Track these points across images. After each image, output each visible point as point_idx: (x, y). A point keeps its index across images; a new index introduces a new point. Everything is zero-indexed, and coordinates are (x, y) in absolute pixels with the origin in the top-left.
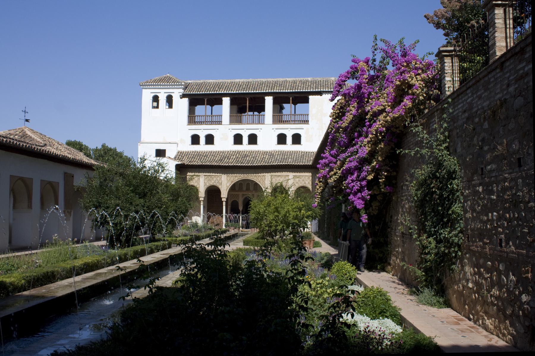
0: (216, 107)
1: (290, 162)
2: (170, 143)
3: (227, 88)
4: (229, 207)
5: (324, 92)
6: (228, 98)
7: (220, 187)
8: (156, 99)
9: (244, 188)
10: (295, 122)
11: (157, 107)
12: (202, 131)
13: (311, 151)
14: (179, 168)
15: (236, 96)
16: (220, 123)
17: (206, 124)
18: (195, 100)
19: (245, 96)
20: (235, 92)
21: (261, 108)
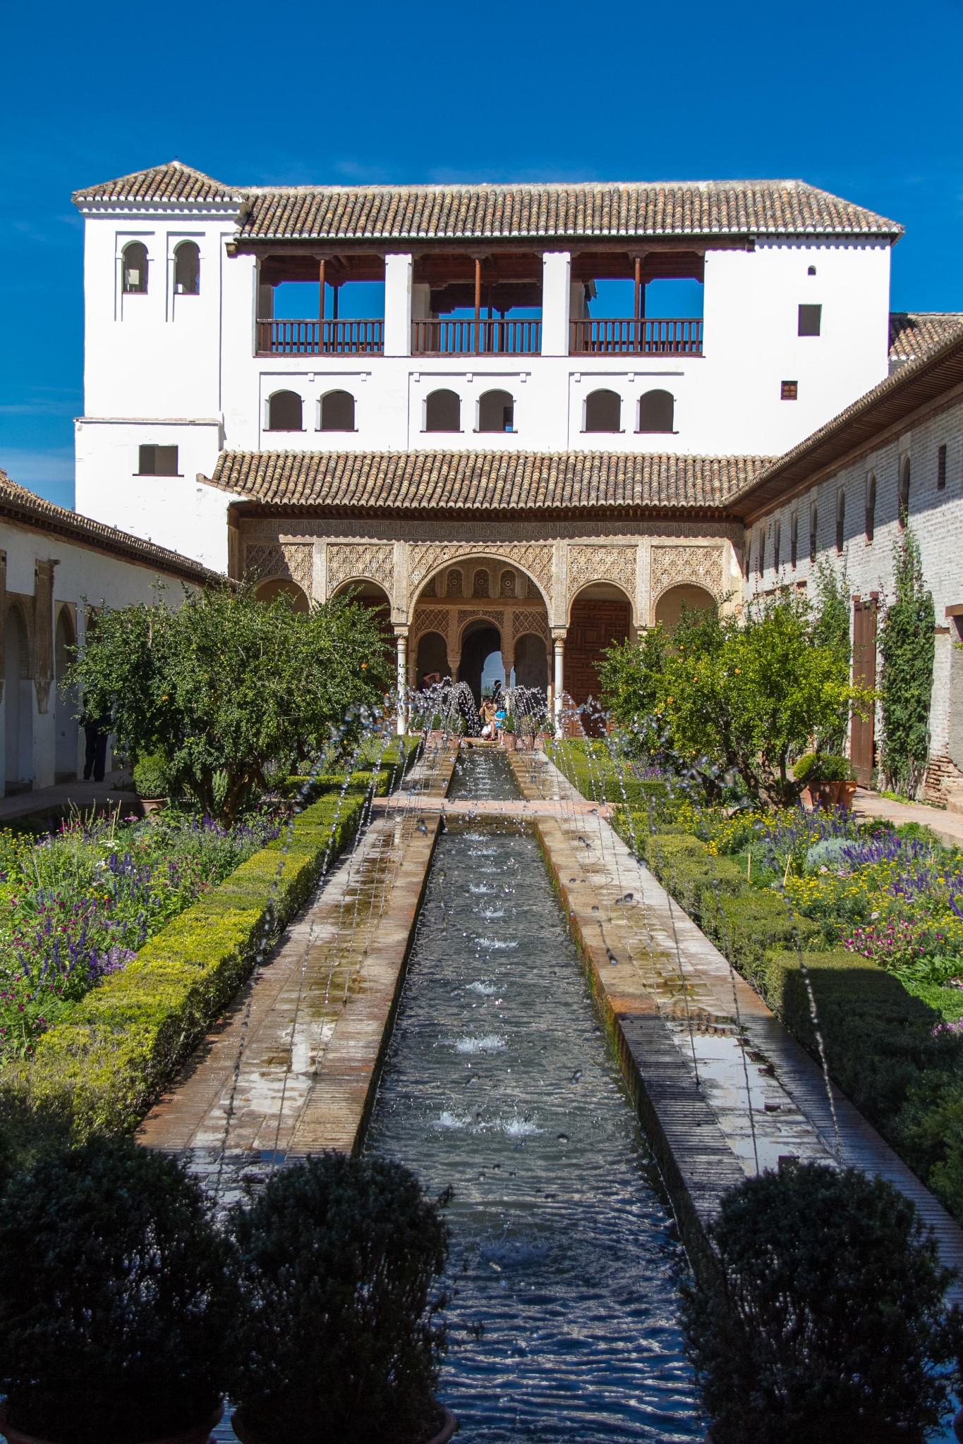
0: (348, 288)
1: (639, 495)
2: (192, 423)
3: (401, 217)
4: (413, 656)
5: (759, 235)
6: (408, 258)
7: (386, 586)
8: (135, 256)
9: (467, 591)
10: (644, 347)
11: (142, 288)
12: (311, 377)
13: (712, 456)
14: (241, 516)
15: (437, 251)
16: (374, 346)
17: (320, 354)
18: (279, 264)
19: (471, 251)
20: (431, 234)
21: (533, 296)
